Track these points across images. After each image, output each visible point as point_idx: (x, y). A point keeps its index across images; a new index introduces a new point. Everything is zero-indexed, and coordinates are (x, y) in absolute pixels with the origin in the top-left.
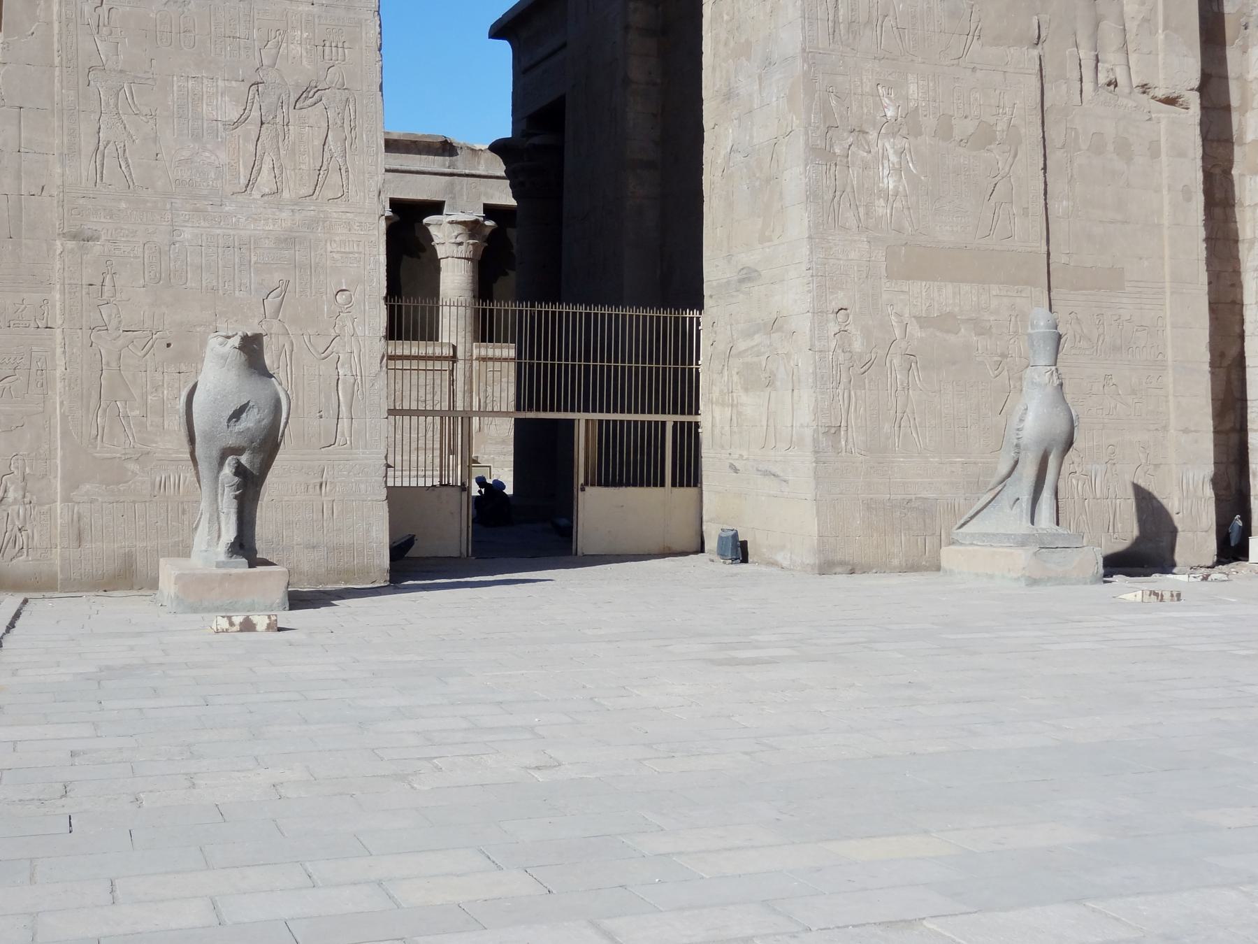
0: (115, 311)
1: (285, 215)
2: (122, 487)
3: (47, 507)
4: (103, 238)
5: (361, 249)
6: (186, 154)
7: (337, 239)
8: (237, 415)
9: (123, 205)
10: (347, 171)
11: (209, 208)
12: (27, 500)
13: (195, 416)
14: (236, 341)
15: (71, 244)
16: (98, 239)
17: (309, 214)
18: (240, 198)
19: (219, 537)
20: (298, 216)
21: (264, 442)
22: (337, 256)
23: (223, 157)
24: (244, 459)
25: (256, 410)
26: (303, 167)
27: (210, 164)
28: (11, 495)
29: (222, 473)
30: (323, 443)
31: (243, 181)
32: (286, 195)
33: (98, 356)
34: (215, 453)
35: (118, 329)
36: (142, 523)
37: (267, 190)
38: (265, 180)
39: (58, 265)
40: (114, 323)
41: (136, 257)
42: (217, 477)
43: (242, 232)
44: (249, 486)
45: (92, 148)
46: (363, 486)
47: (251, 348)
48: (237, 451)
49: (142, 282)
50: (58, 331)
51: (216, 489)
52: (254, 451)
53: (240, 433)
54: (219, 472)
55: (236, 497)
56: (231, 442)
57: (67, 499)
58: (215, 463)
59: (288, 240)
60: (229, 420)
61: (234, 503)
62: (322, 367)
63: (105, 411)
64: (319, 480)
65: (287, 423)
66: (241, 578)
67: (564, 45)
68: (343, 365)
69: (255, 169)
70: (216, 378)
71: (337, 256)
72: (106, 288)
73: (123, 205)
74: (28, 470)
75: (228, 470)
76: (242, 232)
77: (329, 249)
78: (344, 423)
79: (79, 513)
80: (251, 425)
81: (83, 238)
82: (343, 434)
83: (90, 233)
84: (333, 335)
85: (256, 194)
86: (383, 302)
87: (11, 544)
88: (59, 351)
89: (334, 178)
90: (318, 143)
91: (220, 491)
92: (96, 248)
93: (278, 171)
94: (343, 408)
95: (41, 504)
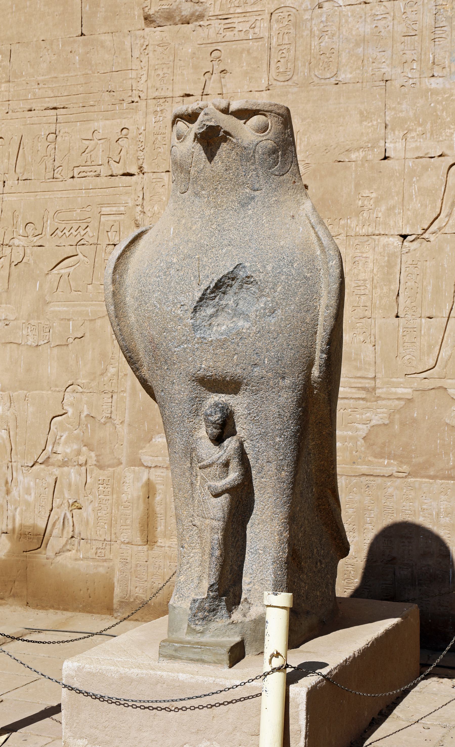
49: (264, 83)
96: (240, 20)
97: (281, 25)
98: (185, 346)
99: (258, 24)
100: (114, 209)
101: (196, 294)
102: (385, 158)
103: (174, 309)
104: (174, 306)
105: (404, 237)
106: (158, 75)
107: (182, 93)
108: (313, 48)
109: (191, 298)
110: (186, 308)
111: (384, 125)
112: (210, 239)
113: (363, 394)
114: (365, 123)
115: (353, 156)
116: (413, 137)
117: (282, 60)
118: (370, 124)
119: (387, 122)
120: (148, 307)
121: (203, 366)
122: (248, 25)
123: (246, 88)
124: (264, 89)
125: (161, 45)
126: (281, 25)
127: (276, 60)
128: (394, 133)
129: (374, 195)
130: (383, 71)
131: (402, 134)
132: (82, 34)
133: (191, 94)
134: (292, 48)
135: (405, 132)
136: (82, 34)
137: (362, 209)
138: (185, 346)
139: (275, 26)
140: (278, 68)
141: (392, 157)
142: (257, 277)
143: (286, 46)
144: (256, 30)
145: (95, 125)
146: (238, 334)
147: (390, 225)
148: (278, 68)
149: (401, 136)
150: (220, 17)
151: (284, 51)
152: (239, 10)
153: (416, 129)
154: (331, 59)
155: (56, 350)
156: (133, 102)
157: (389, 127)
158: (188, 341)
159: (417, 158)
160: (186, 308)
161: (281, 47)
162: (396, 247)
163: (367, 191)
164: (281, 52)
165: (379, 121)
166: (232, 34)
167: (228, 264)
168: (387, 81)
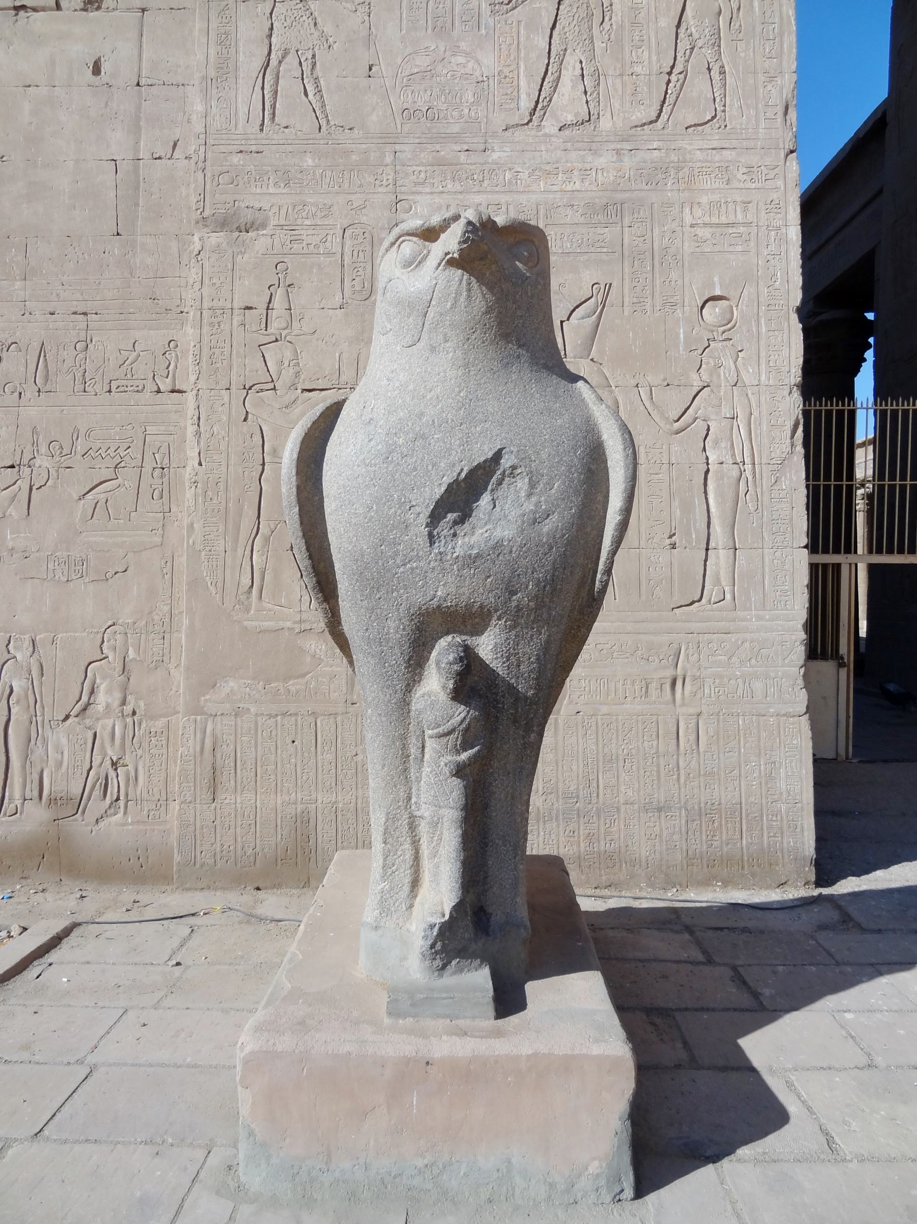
0: (288, 354)
1: (604, 160)
2: (294, 685)
3: (160, 723)
4: (273, 222)
5: (750, 217)
6: (422, 62)
7: (704, 200)
8: (460, 498)
9: (309, 161)
10: (722, 72)
11: (463, 157)
12: (128, 709)
13: (330, 506)
14: (451, 241)
15: (215, 239)
16: (263, 226)
17: (648, 156)
18: (520, 135)
19: (415, 883)
20: (628, 162)
21: (550, 589)
22: (703, 232)
23: (489, 62)
24: (488, 646)
25: (522, 484)
26: (638, 69)
27: (466, 76)
28: (102, 698)
29: (420, 691)
30: (677, 600)
31: (526, 104)
32: (605, 124)
33: (257, 439)
34: (396, 628)
35: (294, 386)
36: (330, 757)
37: (570, 118)
38: (567, 100)
39: (193, 275)
40: (288, 374)
41: (330, 254)
42: (404, 704)
43: (523, 198)
44: (503, 724)
45: (258, 63)
46: (758, 686)
47: (505, 266)
48: (469, 620)
49: (338, 299)
50: (190, 397)
51: (404, 738)
52: (516, 620)
53: (471, 561)
54: (409, 689)
55: (460, 771)
56: (445, 590)
57: (196, 710)
58: (397, 658)
59: (611, 209)
60: (435, 517)
61: (455, 790)
62: (675, 448)
63: (267, 540)
64: (669, 673)
65: (623, 526)
66: (470, 1075)
67: (880, 192)
68: (716, 442)
69: (548, 79)
70: (406, 385)
71: (703, 232)
72: (274, 314)
73: (309, 161)
74: (131, 654)
75: (435, 683)
76: (523, 198)
77: (688, 220)
78: (720, 558)
79: (214, 735)
80: (505, 532)
81: (238, 225)
82: (717, 581)
83: (248, 216)
84: (697, 384)
85: (550, 126)
86: (794, 317)
87: (97, 792)
88: (191, 430)
89: (698, 86)
90: (666, 22)
91: (413, 751)
92: (260, 242)
93: (591, 81)
94: (718, 528)
95: (153, 718)
96: (309, 232)
97: (356, 242)
98: (414, 565)
99: (329, 238)
100: (163, 428)
101: (436, 490)
103: (399, 511)
104: (400, 508)
106: (214, 284)
107: (243, 305)
109: (427, 495)
110: (418, 509)
112: (457, 411)
120: (356, 509)
121: (439, 593)
122: (319, 239)
126: (356, 242)
132: (118, 234)
136: (118, 234)
138: (414, 565)
139: (348, 243)
140: (353, 286)
143: (361, 264)
144: (328, 244)
145: (137, 334)
146: (494, 548)
148: (353, 286)
150: (286, 228)
152: (307, 222)
155: (91, 587)
156: (182, 312)
158: (418, 558)
160: (418, 509)
166: (301, 246)
167: (486, 447)
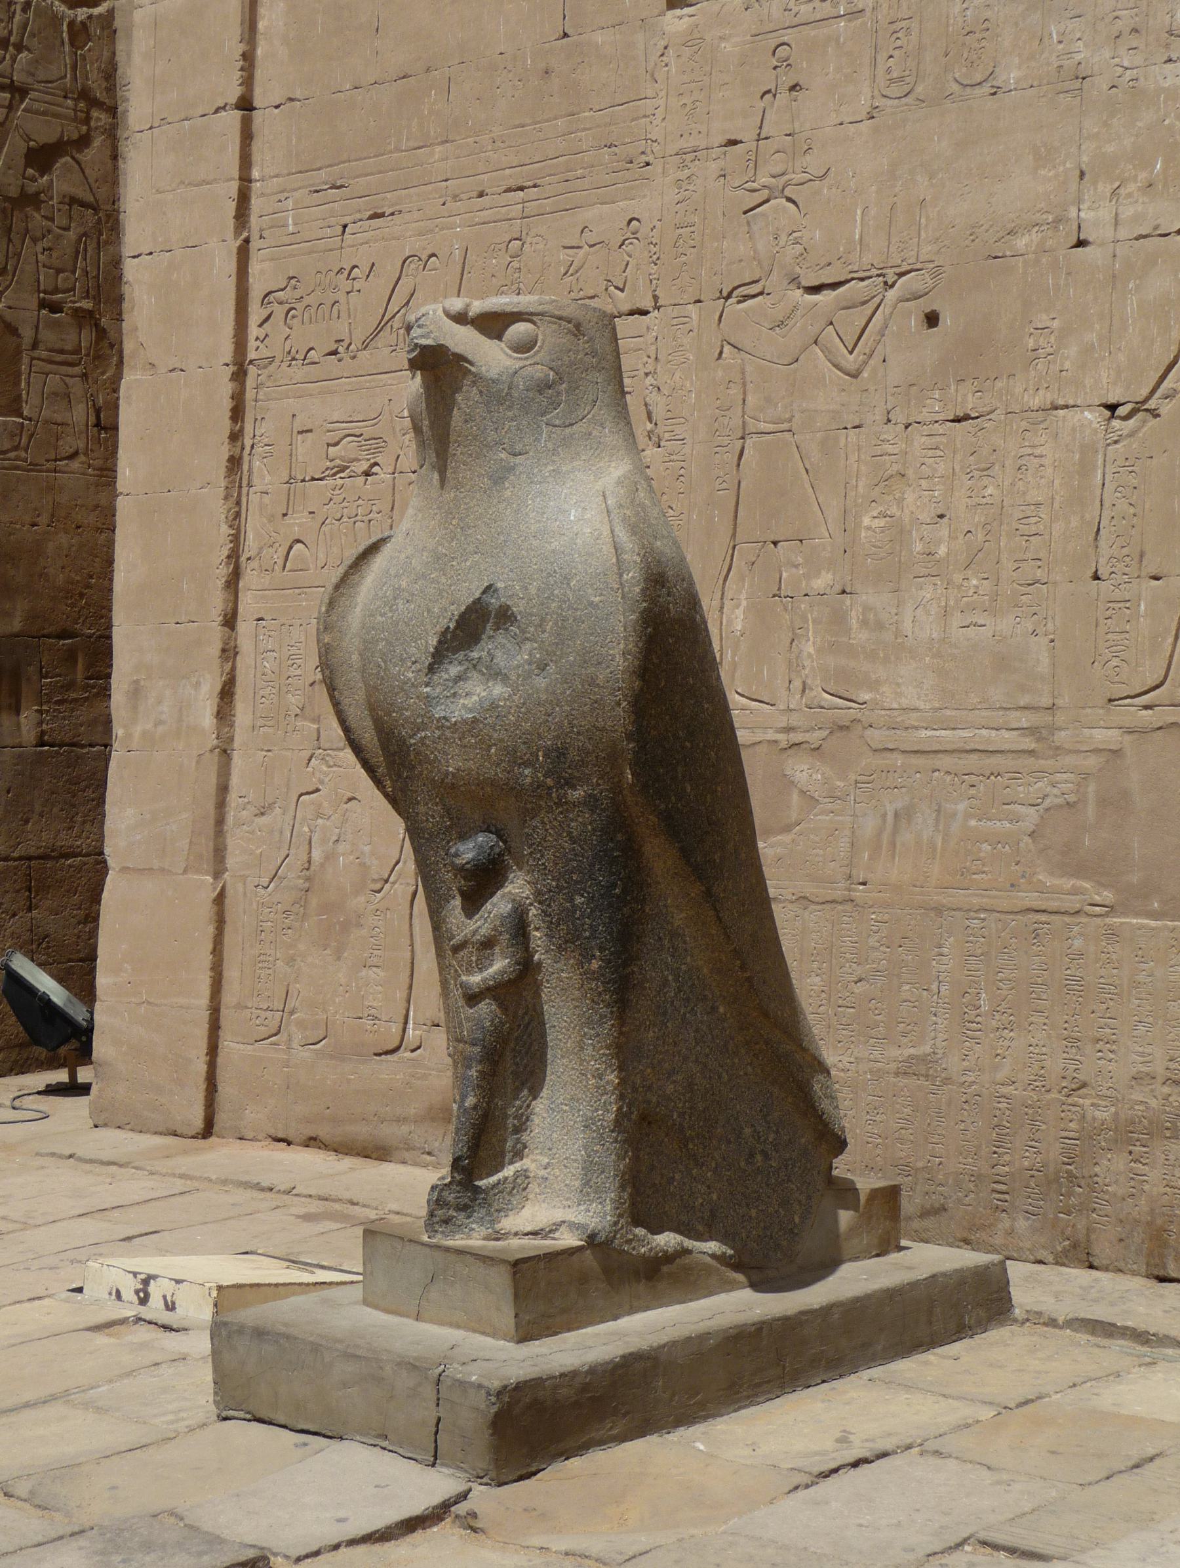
102: (1081, 243)
105: (1112, 408)
108: (952, 21)
111: (1078, 173)
113: (1028, 743)
114: (1042, 172)
115: (1021, 242)
116: (1130, 195)
117: (896, 53)
118: (1051, 174)
119: (1084, 167)
123: (834, 119)
124: (864, 115)
125: (689, 44)
127: (886, 55)
128: (1096, 189)
129: (1056, 324)
130: (1078, 57)
131: (1109, 188)
133: (739, 139)
134: (914, 25)
135: (1117, 184)
137: (1034, 355)
140: (889, 70)
141: (1091, 240)
142: (518, 608)
143: (904, 24)
147: (1085, 386)
148: (889, 70)
149: (1108, 194)
151: (899, 35)
153: (1136, 176)
154: (984, 43)
157: (1087, 177)
159: (1137, 239)
161: (894, 27)
162: (1095, 431)
163: (1044, 317)
164: (895, 35)
165: (1068, 165)
168: (1084, 78)
